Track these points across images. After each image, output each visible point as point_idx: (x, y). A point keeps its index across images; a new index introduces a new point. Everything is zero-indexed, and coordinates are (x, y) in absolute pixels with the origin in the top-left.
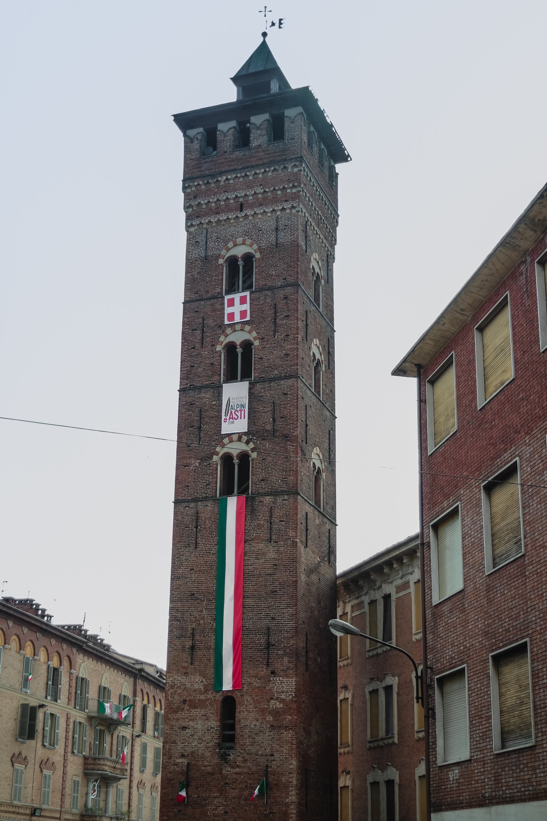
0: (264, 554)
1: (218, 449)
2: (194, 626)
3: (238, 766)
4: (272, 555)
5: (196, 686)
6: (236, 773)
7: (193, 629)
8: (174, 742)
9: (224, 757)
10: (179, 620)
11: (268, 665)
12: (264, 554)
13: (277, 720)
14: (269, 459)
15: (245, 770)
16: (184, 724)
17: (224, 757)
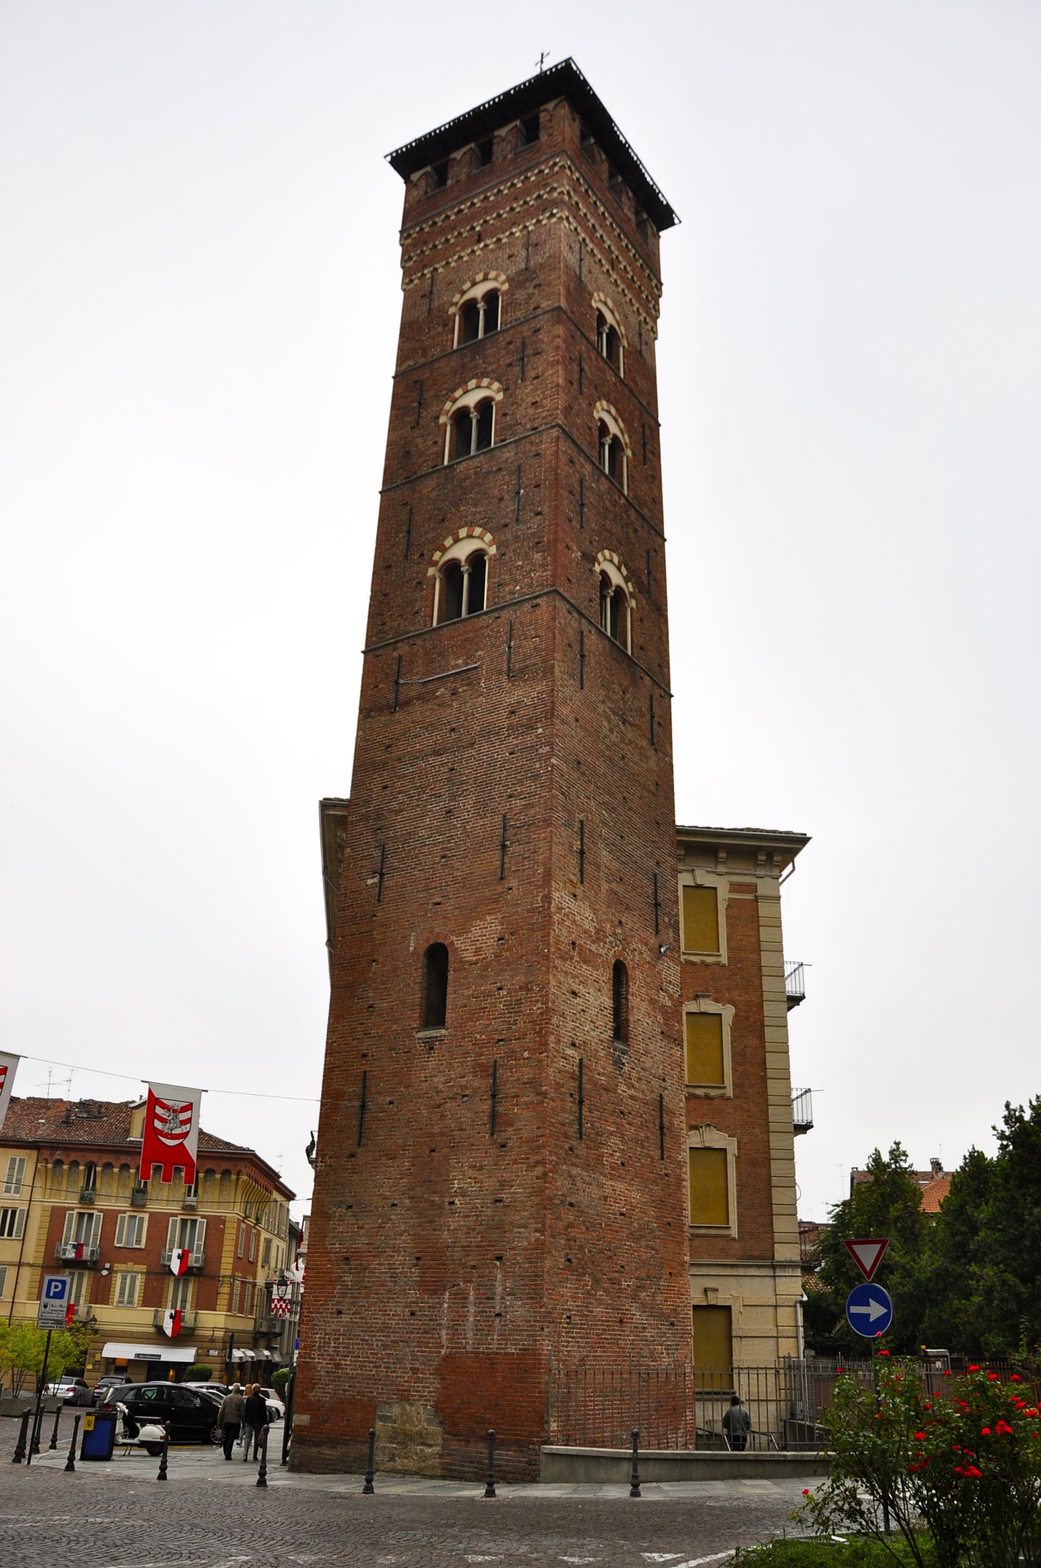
0: (648, 758)
1: (600, 556)
2: (582, 816)
3: (633, 1087)
4: (652, 763)
5: (587, 925)
6: (632, 1097)
7: (582, 822)
8: (563, 1015)
9: (618, 1064)
10: (563, 794)
11: (657, 932)
12: (648, 758)
13: (666, 1024)
14: (646, 624)
15: (641, 1096)
16: (575, 987)
17: (618, 1064)
